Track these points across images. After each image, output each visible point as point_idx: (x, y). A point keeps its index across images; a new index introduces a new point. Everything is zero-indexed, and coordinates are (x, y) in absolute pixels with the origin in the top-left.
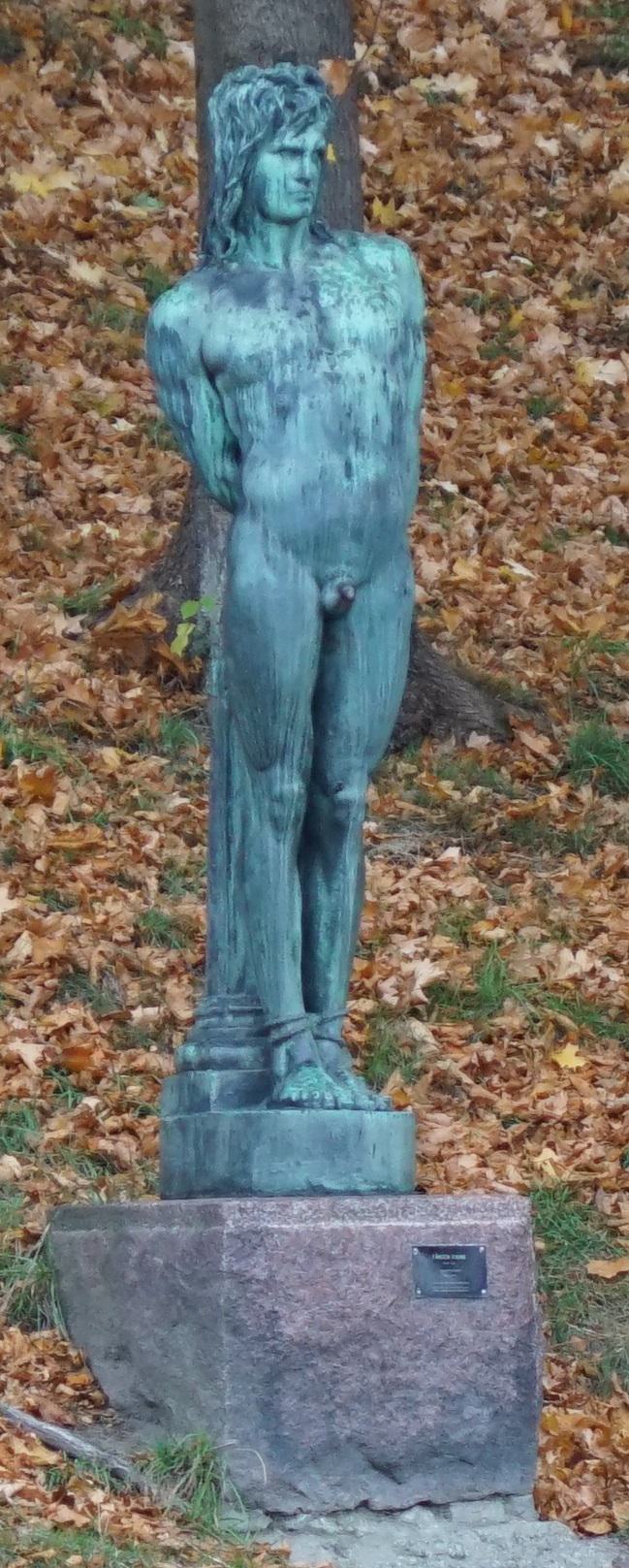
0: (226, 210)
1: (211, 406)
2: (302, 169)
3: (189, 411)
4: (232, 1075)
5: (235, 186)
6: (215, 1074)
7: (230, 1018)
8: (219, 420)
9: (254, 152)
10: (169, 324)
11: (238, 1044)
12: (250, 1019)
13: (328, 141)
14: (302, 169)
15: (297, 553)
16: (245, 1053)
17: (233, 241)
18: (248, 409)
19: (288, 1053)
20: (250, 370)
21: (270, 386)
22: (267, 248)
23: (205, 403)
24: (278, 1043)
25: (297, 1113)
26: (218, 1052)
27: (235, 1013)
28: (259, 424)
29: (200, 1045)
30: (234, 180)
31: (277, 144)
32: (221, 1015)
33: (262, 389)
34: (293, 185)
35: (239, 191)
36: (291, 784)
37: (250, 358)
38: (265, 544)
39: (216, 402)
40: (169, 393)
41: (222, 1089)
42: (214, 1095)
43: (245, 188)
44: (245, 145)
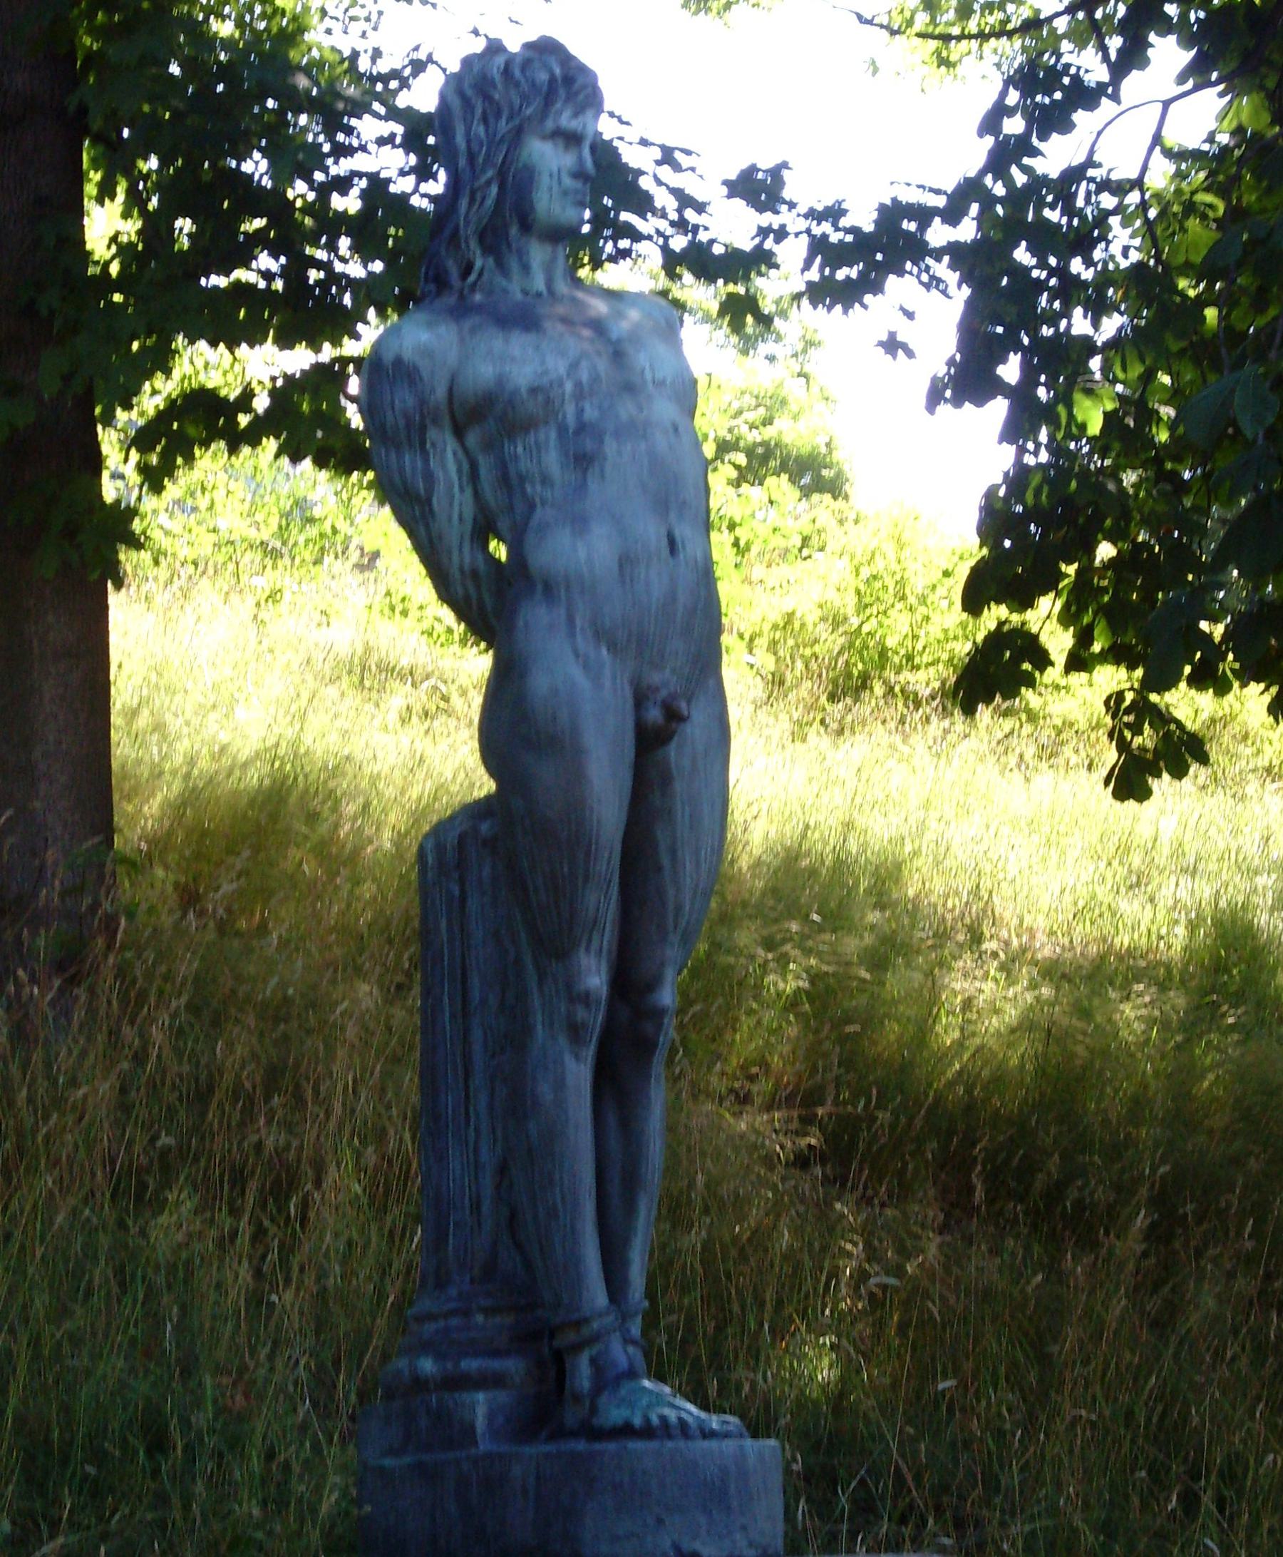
0: (473, 218)
1: (459, 471)
2: (580, 160)
3: (429, 477)
4: (502, 1397)
5: (489, 183)
6: (481, 1396)
7: (480, 1318)
8: (469, 492)
9: (518, 135)
10: (407, 355)
11: (496, 1353)
12: (508, 1319)
13: (123, 515)
14: (580, 160)
15: (613, 647)
16: (513, 1366)
17: (478, 263)
18: (525, 465)
19: (593, 1361)
20: (532, 407)
21: (562, 429)
22: (526, 268)
23: (452, 467)
24: (578, 1348)
25: (653, 1445)
26: (471, 1365)
27: (487, 1311)
28: (546, 480)
29: (440, 1356)
30: (490, 173)
31: (550, 125)
32: (466, 1313)
33: (550, 435)
34: (568, 182)
35: (494, 190)
36: (595, 976)
37: (534, 391)
38: (572, 634)
39: (466, 467)
40: (400, 455)
41: (491, 1417)
42: (480, 1423)
43: (502, 187)
44: (503, 126)
